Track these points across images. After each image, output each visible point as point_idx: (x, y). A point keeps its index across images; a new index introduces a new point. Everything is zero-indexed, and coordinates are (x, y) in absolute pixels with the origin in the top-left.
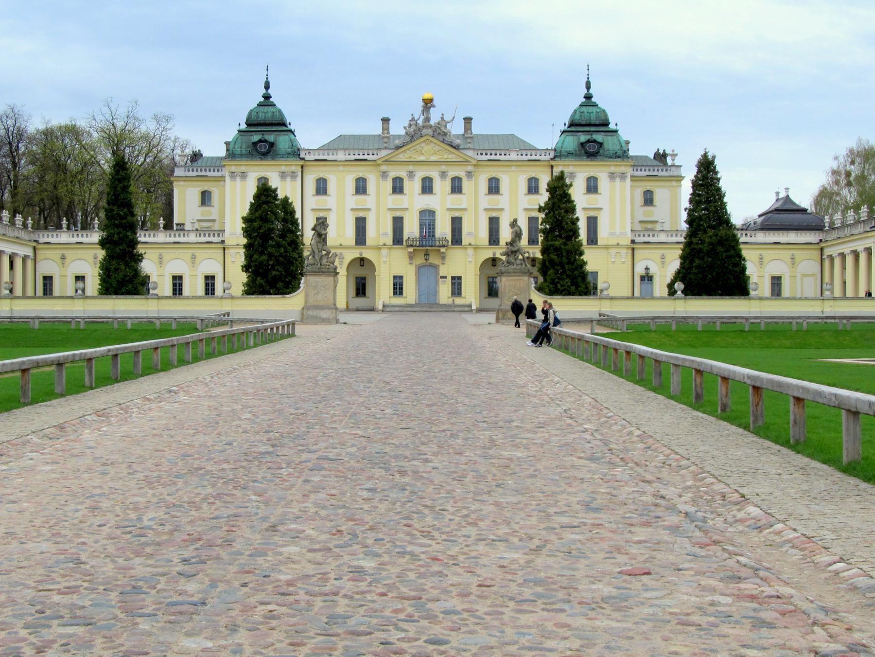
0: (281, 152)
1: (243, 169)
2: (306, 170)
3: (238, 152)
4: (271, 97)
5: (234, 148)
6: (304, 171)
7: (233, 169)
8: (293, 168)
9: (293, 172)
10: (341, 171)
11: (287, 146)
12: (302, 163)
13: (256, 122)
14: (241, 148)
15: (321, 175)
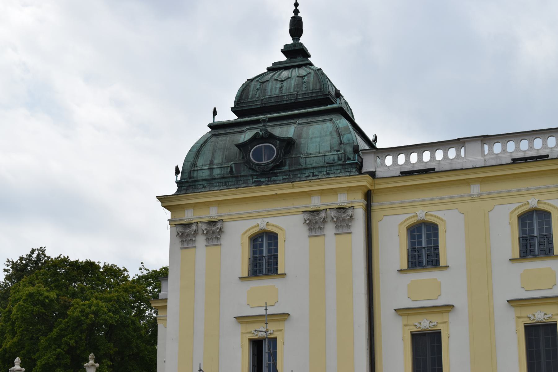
0: (310, 162)
1: (213, 213)
2: (377, 202)
3: (204, 174)
4: (310, 56)
5: (194, 164)
6: (375, 206)
7: (188, 216)
8: (342, 200)
9: (341, 209)
10: (476, 198)
11: (326, 147)
12: (365, 182)
13: (258, 105)
14: (212, 163)
15: (421, 214)
